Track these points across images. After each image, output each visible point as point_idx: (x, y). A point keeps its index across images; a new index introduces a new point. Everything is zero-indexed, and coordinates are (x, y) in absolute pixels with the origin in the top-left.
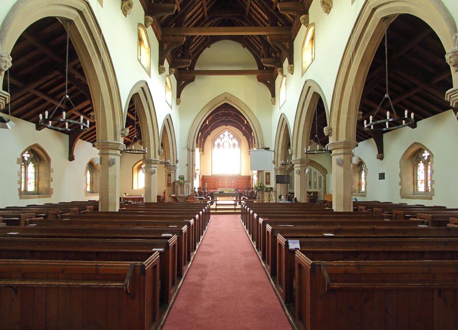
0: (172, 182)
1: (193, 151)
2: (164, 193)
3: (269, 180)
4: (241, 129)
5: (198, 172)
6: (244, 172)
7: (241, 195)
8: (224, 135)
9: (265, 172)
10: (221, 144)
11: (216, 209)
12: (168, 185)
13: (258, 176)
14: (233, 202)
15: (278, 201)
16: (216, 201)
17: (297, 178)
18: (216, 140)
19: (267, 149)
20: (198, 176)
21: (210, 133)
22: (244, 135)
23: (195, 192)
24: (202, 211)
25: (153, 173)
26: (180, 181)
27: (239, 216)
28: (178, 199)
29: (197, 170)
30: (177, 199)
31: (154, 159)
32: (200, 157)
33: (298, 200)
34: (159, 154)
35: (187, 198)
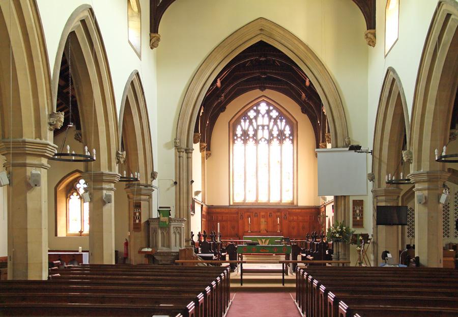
0: (144, 220)
1: (189, 151)
2: (127, 244)
3: (362, 218)
4: (297, 99)
5: (199, 198)
6: (305, 200)
7: (296, 250)
8: (258, 112)
9: (351, 199)
10: (251, 133)
11: (242, 281)
12: (134, 228)
13: (335, 208)
14: (279, 267)
15: (381, 263)
16: (242, 263)
17: (420, 213)
18: (238, 122)
19: (356, 148)
20: (198, 208)
21: (225, 108)
22: (304, 111)
23: (193, 243)
24: (211, 286)
25: (105, 202)
26: (162, 219)
27: (293, 296)
28: (157, 258)
29: (197, 193)
30: (154, 258)
31: (107, 172)
32: (203, 162)
33: (423, 261)
34: (119, 162)
35: (177, 256)
